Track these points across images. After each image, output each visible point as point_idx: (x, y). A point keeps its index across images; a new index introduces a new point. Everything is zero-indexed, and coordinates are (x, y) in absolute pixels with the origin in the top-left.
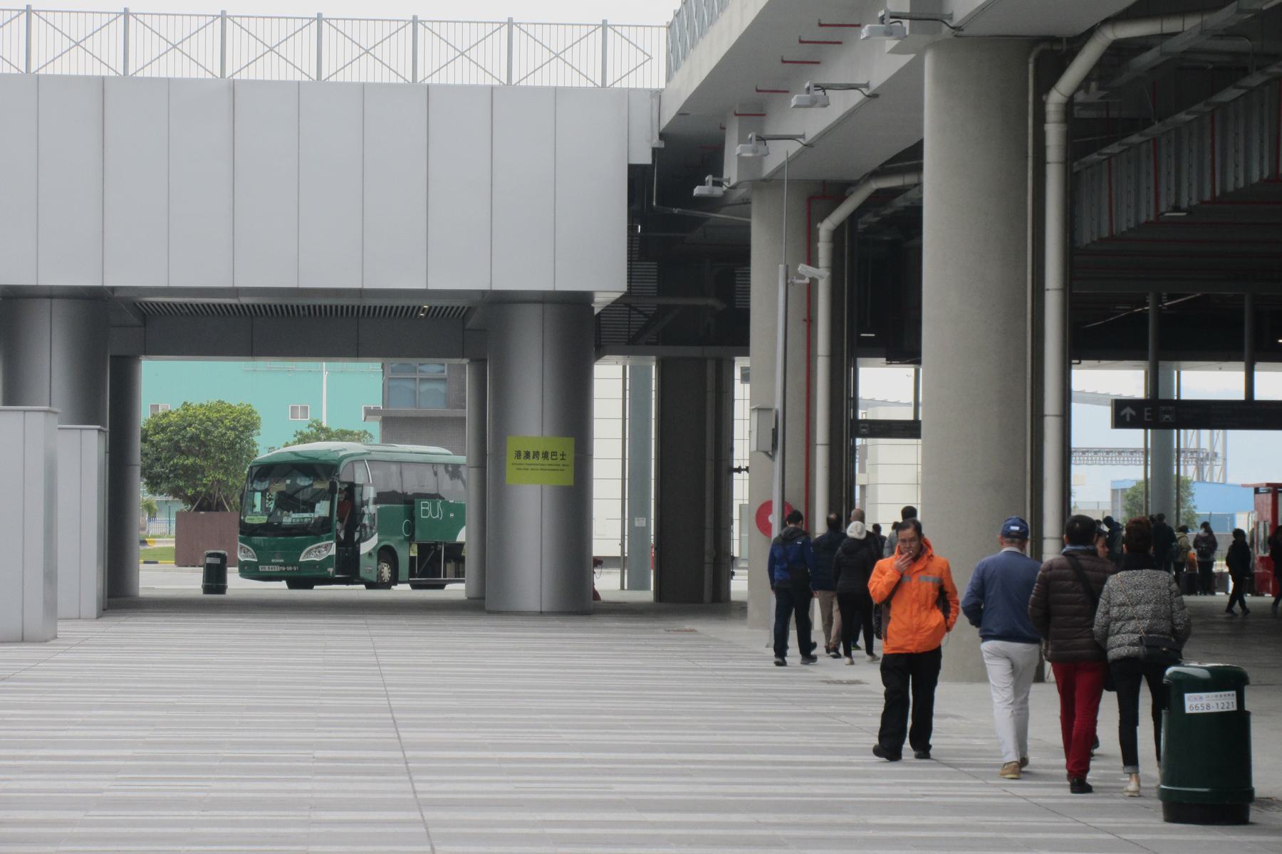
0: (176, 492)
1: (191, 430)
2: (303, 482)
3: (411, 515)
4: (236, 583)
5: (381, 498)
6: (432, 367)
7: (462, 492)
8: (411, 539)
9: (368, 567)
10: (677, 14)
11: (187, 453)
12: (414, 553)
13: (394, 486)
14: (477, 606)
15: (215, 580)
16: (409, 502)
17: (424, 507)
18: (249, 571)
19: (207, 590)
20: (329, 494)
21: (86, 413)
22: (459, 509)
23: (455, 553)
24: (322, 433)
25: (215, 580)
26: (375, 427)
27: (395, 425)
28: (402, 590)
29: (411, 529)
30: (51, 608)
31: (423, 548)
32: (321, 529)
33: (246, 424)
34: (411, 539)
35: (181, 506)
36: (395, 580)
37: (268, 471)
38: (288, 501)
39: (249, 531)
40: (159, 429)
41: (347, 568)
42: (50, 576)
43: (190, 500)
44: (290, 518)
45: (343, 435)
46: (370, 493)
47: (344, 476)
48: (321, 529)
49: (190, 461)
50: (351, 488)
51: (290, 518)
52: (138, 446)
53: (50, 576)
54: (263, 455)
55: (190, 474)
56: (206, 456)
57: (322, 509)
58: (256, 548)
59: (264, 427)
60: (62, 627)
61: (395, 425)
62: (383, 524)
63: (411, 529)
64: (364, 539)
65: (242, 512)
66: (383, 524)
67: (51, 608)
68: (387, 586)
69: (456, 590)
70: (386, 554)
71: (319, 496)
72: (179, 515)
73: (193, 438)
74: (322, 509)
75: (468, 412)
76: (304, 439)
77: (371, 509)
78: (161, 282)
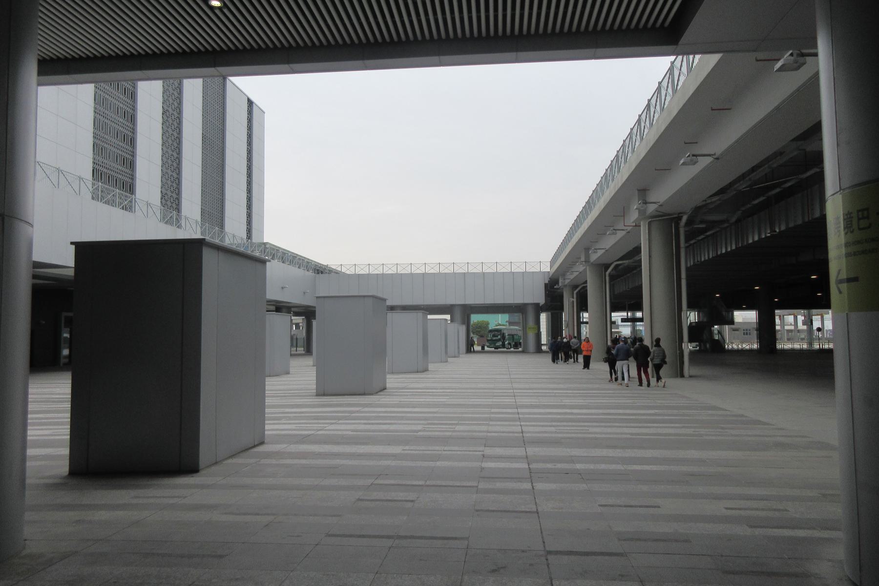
0: (477, 334)
1: (479, 325)
2: (496, 333)
3: (513, 337)
4: (486, 348)
5: (508, 335)
6: (516, 314)
7: (520, 333)
8: (513, 342)
9: (507, 346)
10: (557, 250)
11: (478, 328)
12: (514, 343)
13: (510, 333)
14: (523, 352)
15: (483, 348)
16: (513, 335)
17: (515, 336)
18: (488, 347)
19: (482, 349)
20: (500, 335)
21: (463, 323)
22: (521, 337)
23: (520, 344)
24: (500, 325)
25: (483, 348)
26: (508, 324)
27: (511, 323)
28: (512, 349)
29: (513, 340)
30: (459, 353)
31: (515, 343)
32: (499, 340)
33: (488, 324)
34: (513, 342)
35: (478, 337)
36: (511, 348)
37: (491, 331)
38: (494, 336)
39: (488, 340)
40: (474, 325)
41: (503, 346)
42: (459, 348)
43: (479, 336)
44: (494, 338)
45: (503, 325)
46: (507, 334)
47: (503, 332)
48: (499, 340)
49: (479, 330)
50: (504, 334)
51: (494, 338)
52: (471, 327)
53: (459, 348)
54: (490, 328)
55: (479, 332)
56: (481, 329)
57: (499, 337)
58: (490, 343)
59: (490, 324)
60: (461, 355)
61: (511, 323)
62: (509, 339)
63: (513, 340)
64: (506, 341)
65: (487, 337)
66: (509, 339)
67: (459, 353)
68: (510, 349)
69: (520, 349)
70: (509, 344)
71: (499, 335)
72: (478, 338)
73: (480, 326)
74: (499, 337)
75: (521, 321)
76: (497, 326)
77: (507, 337)
78: (474, 303)
